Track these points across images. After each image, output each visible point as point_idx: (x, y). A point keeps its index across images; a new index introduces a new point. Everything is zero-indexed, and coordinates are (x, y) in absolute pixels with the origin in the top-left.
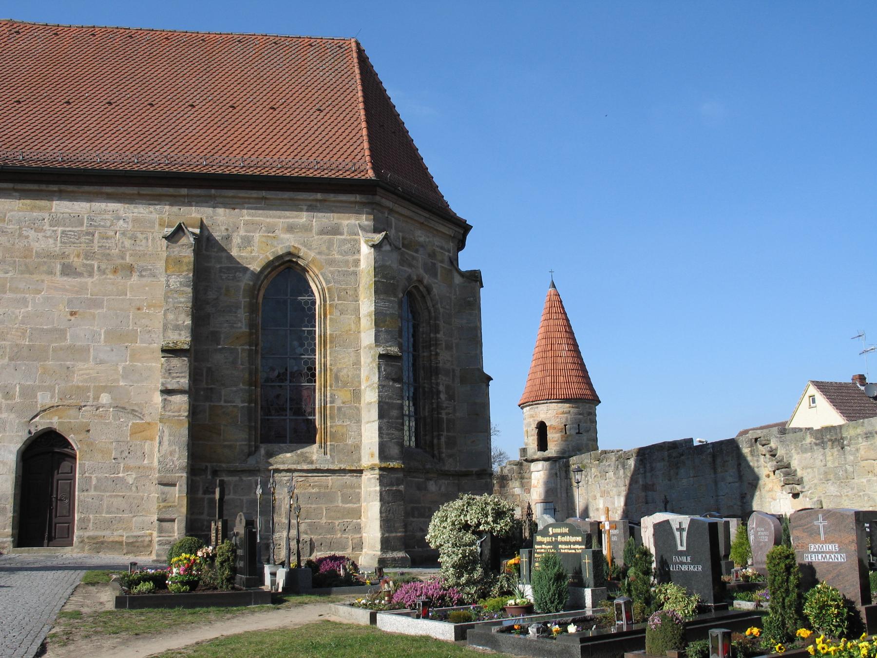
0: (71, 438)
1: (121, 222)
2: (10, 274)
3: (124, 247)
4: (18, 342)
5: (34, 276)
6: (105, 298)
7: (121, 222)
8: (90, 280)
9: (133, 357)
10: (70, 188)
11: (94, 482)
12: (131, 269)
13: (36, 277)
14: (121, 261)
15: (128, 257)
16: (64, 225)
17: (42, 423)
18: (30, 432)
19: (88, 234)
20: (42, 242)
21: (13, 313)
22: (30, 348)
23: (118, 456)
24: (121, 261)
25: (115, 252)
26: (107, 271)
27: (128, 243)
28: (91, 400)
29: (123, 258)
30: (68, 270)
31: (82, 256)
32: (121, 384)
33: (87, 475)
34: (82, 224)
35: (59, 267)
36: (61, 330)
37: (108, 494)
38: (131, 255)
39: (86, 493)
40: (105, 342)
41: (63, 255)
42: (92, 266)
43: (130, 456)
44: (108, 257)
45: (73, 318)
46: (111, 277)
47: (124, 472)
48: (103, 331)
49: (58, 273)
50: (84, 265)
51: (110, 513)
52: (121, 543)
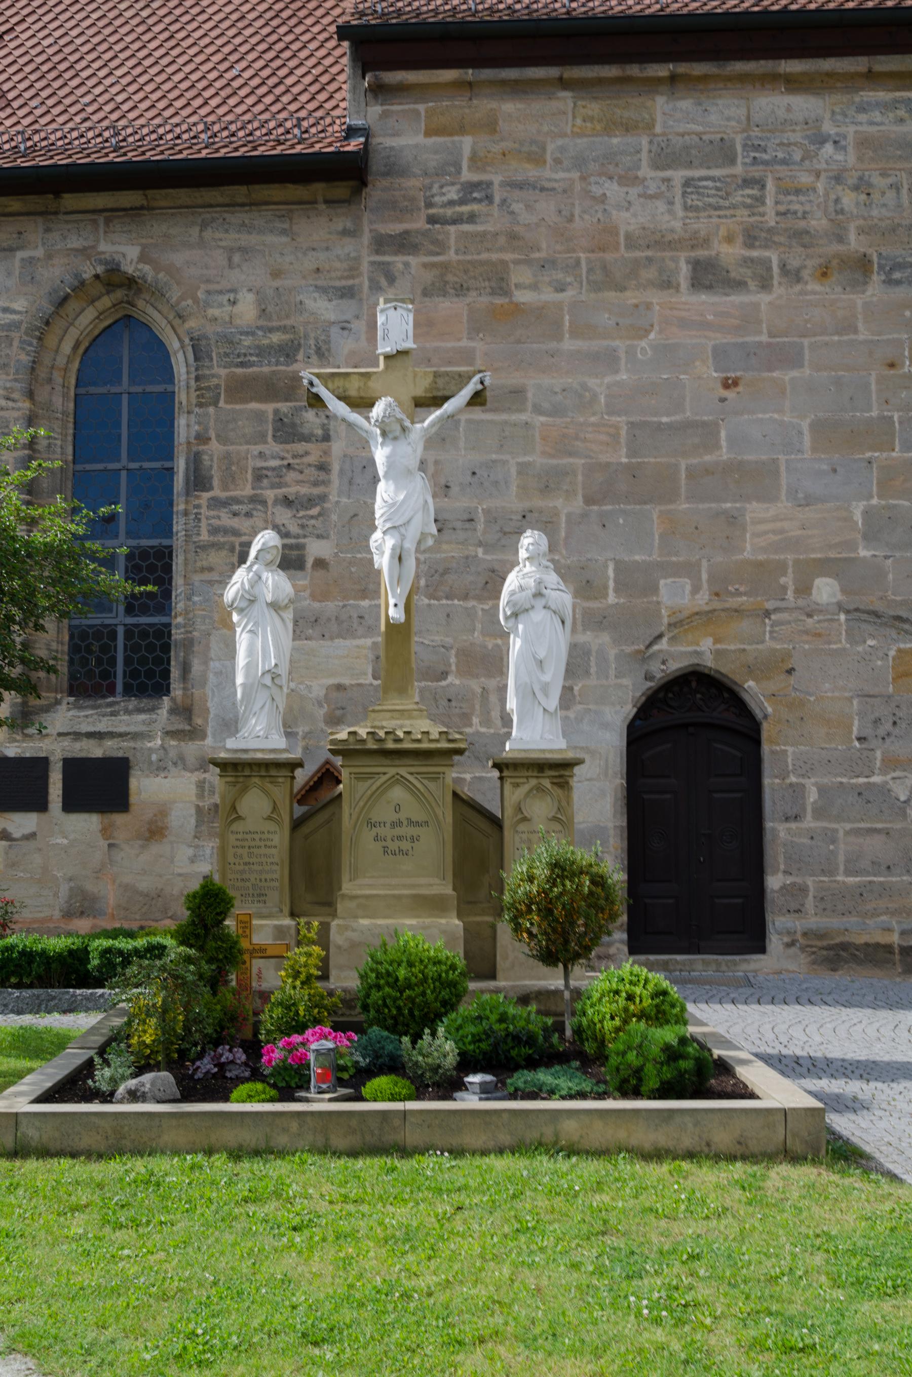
0: (754, 691)
1: (829, 148)
2: (570, 293)
3: (842, 212)
4: (604, 458)
5: (628, 294)
6: (806, 342)
7: (829, 148)
8: (764, 298)
9: (884, 489)
10: (699, 69)
11: (813, 796)
12: (863, 265)
13: (631, 297)
14: (836, 248)
15: (852, 237)
16: (690, 165)
17: (675, 655)
18: (648, 677)
19: (747, 182)
20: (635, 212)
21: (584, 387)
22: (633, 472)
23: (868, 732)
24: (836, 248)
25: (818, 223)
26: (805, 274)
27: (849, 200)
28: (790, 594)
29: (841, 239)
30: (707, 275)
31: (740, 240)
32: (863, 553)
33: (793, 779)
34: (732, 161)
35: (684, 270)
36: (704, 424)
37: (848, 826)
38: (861, 231)
39: (793, 825)
40: (814, 449)
41: (696, 241)
42: (766, 264)
43: (896, 731)
44: (801, 236)
45: (730, 394)
46: (818, 288)
47: (883, 772)
48: (805, 425)
49: (684, 284)
50: (747, 262)
51: (856, 873)
52: (888, 948)
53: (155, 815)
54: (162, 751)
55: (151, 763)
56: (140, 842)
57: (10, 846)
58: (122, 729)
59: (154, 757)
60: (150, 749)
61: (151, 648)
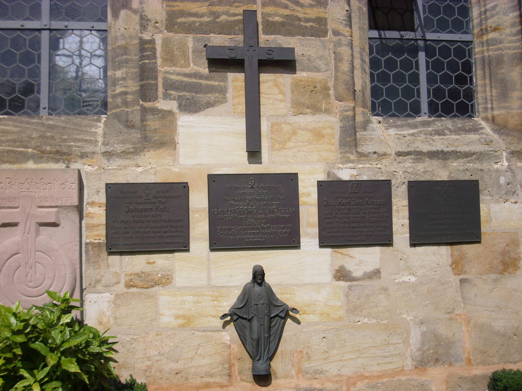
53: (508, 245)
54: (509, 174)
55: (499, 186)
56: (493, 276)
57: (350, 287)
58: (466, 149)
59: (502, 180)
60: (497, 171)
61: (453, 66)
